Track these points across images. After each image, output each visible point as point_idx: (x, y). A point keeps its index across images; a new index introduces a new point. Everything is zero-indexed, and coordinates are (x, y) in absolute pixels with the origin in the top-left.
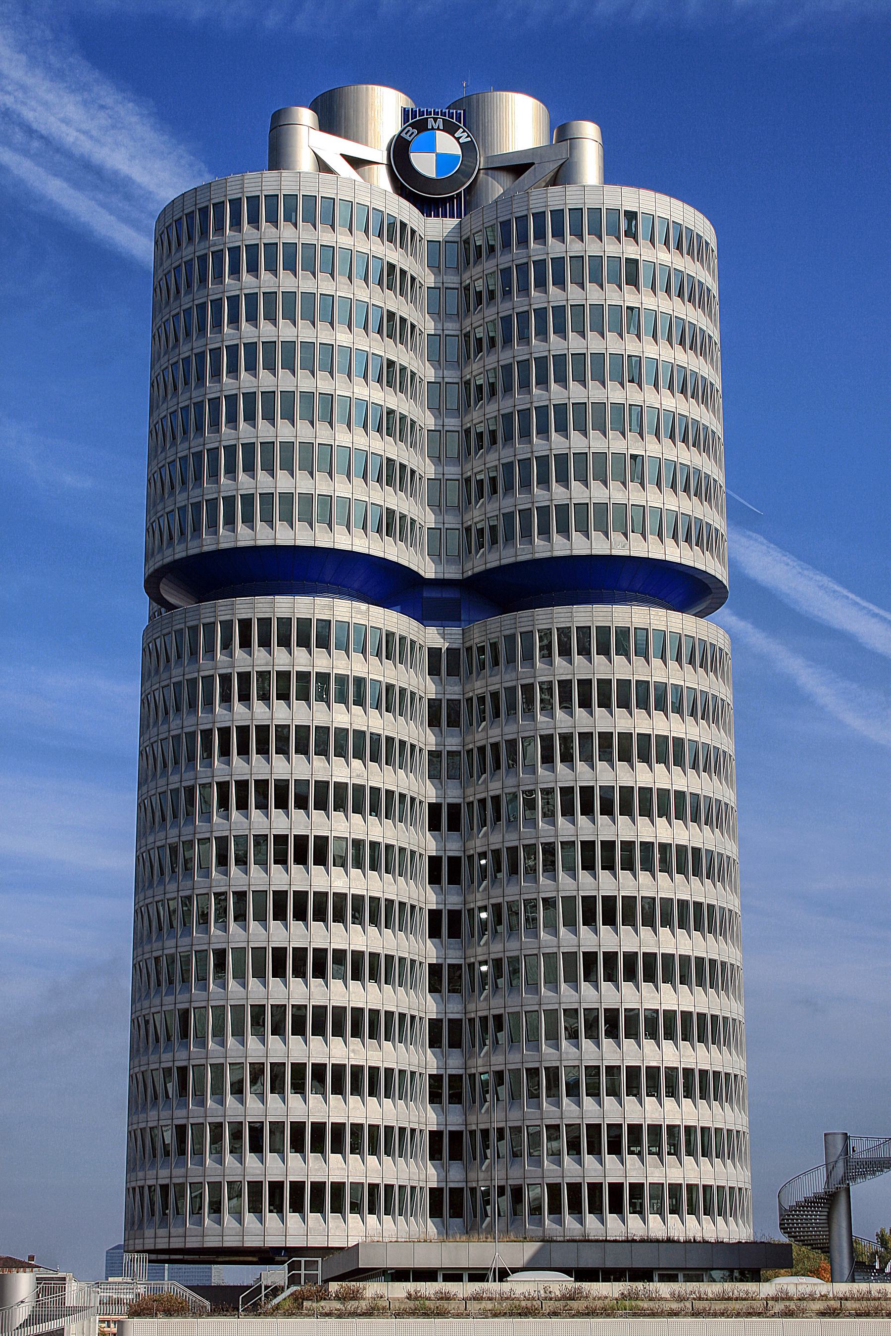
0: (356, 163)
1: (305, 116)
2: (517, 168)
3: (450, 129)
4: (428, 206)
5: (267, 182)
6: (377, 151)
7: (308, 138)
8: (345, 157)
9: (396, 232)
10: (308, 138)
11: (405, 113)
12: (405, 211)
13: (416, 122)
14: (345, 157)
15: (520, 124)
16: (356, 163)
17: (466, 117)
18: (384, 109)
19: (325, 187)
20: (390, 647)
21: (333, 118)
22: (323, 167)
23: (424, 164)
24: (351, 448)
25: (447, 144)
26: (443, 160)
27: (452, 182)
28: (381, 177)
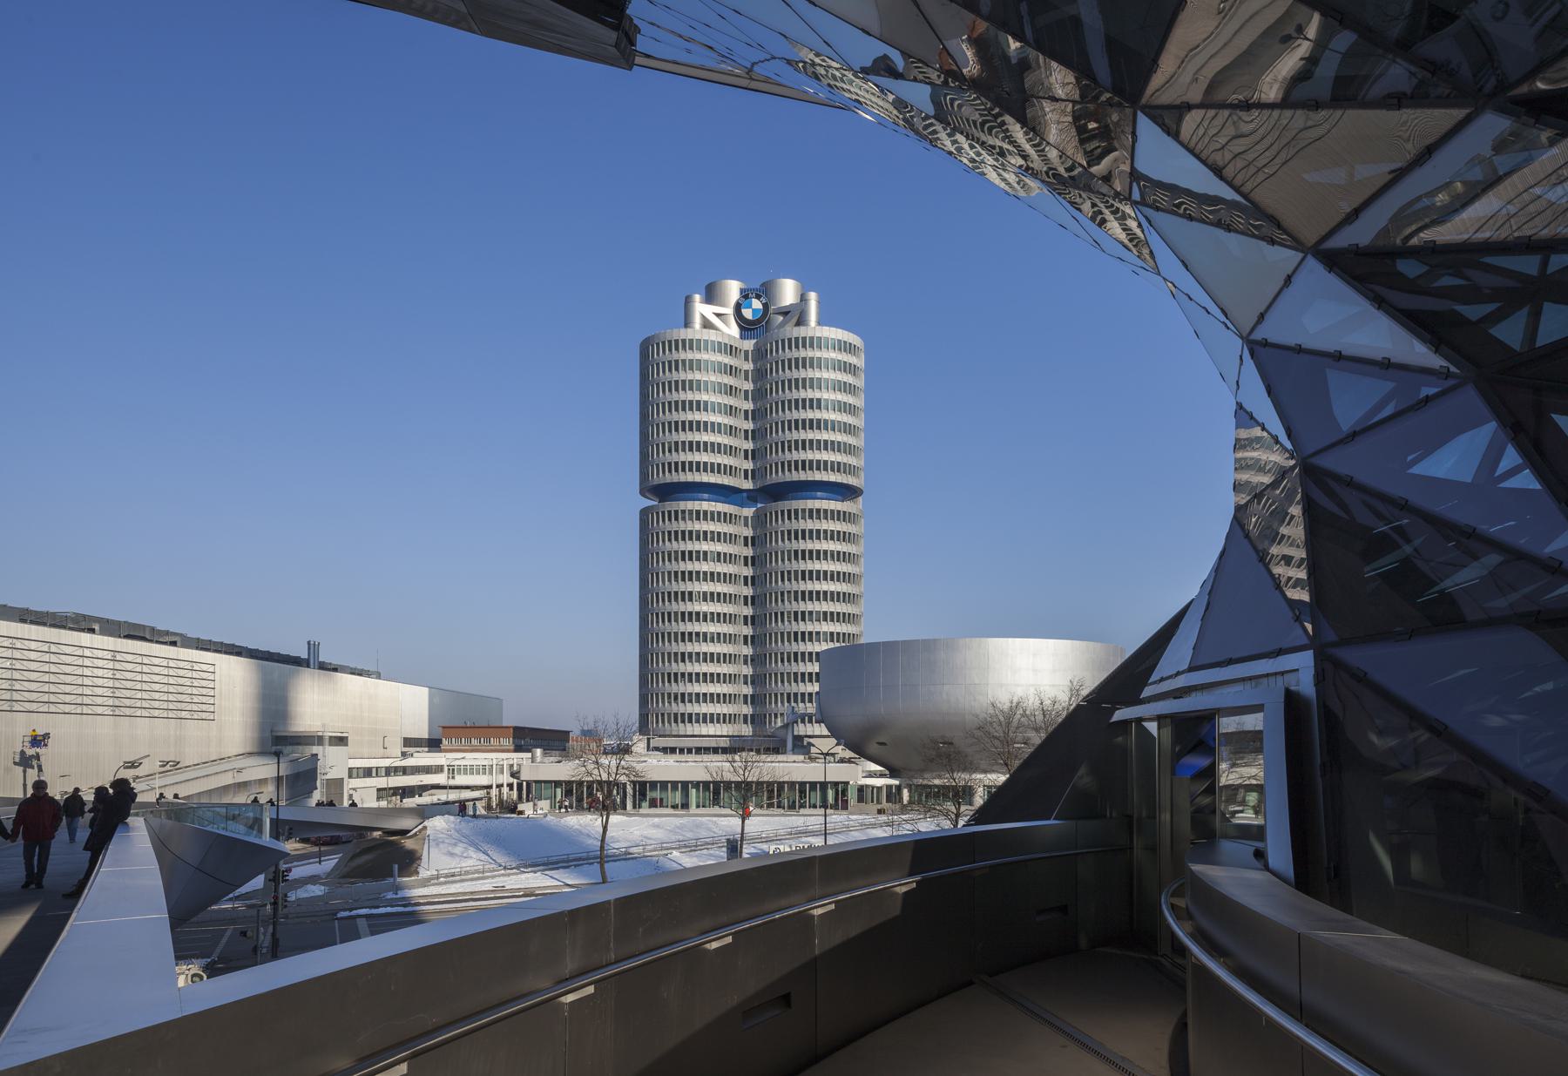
0: (718, 315)
1: (697, 297)
2: (785, 312)
3: (758, 297)
5: (684, 334)
6: (729, 311)
7: (701, 309)
10: (701, 309)
11: (742, 291)
13: (745, 295)
15: (788, 291)
16: (718, 315)
17: (765, 291)
18: (733, 289)
21: (711, 296)
23: (748, 314)
24: (716, 434)
25: (757, 304)
27: (758, 321)
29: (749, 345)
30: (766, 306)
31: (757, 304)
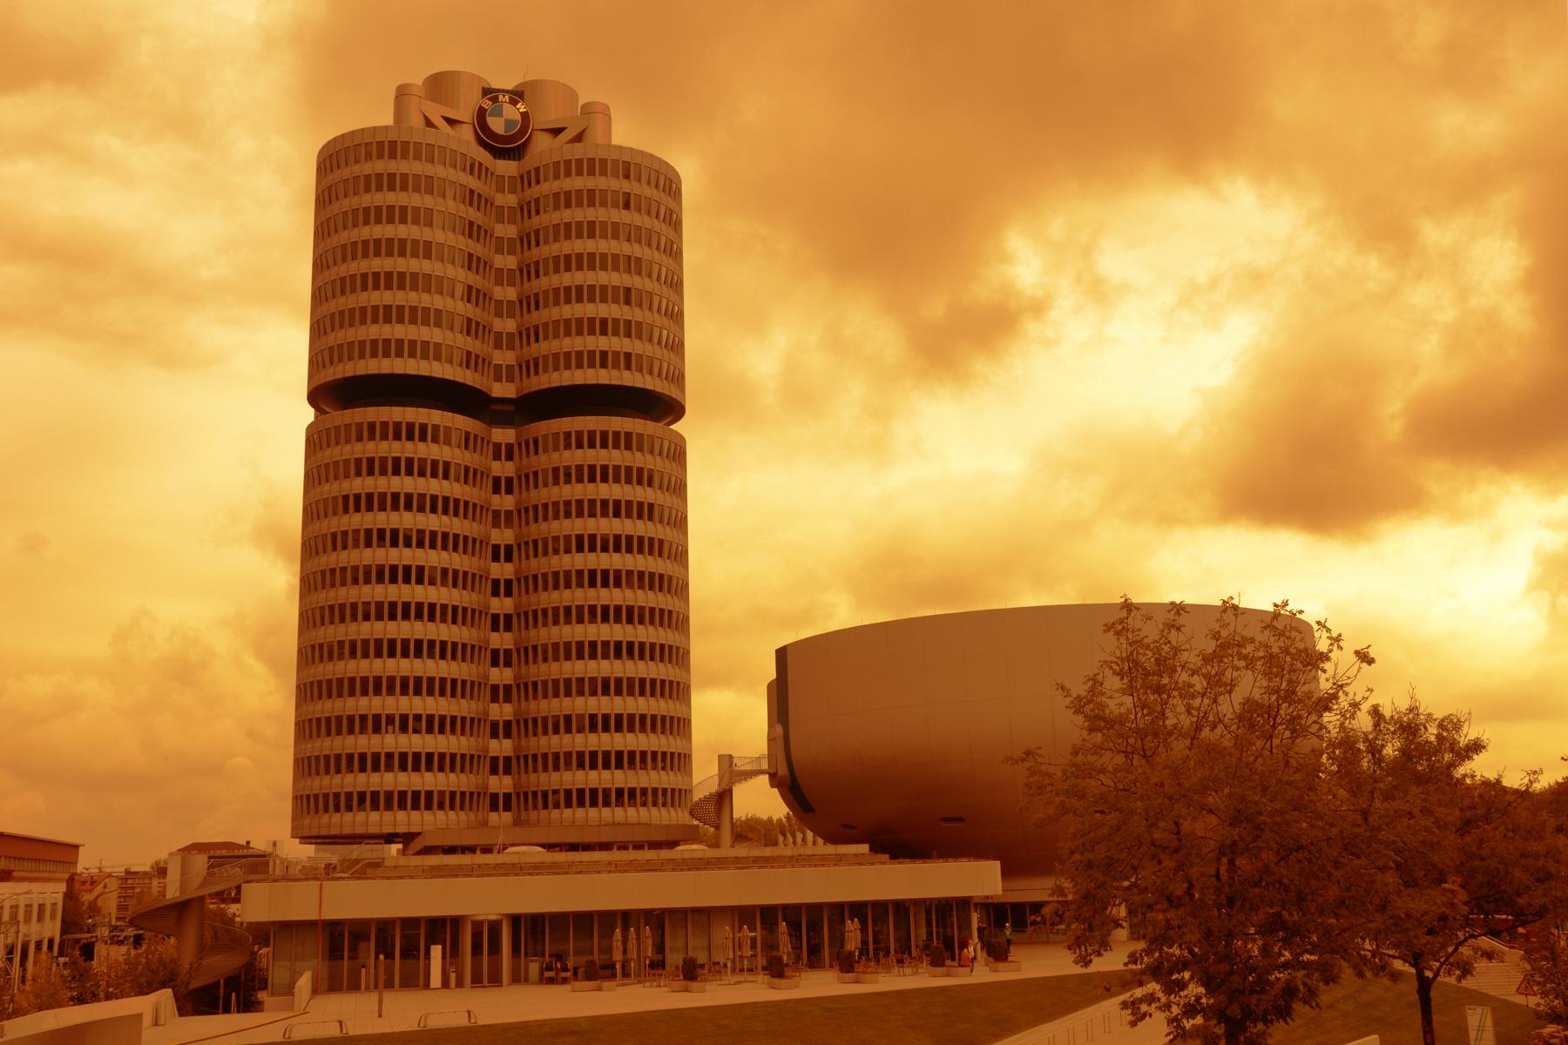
0: (451, 122)
3: (514, 102)
4: (498, 153)
6: (465, 113)
8: (445, 118)
9: (473, 168)
12: (483, 156)
14: (445, 118)
16: (451, 122)
19: (430, 137)
20: (468, 441)
22: (429, 123)
23: (496, 125)
26: (509, 123)
27: (513, 138)
28: (467, 133)
29: (507, 168)
30: (525, 116)
31: (512, 112)
